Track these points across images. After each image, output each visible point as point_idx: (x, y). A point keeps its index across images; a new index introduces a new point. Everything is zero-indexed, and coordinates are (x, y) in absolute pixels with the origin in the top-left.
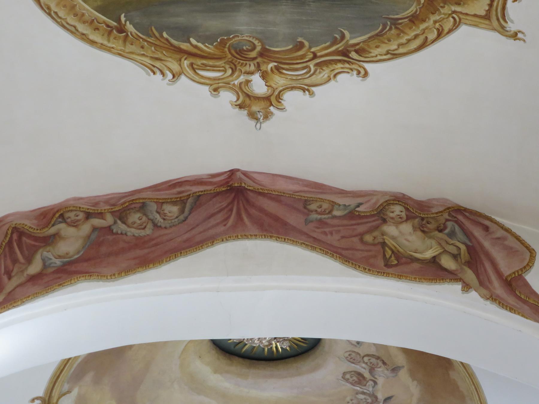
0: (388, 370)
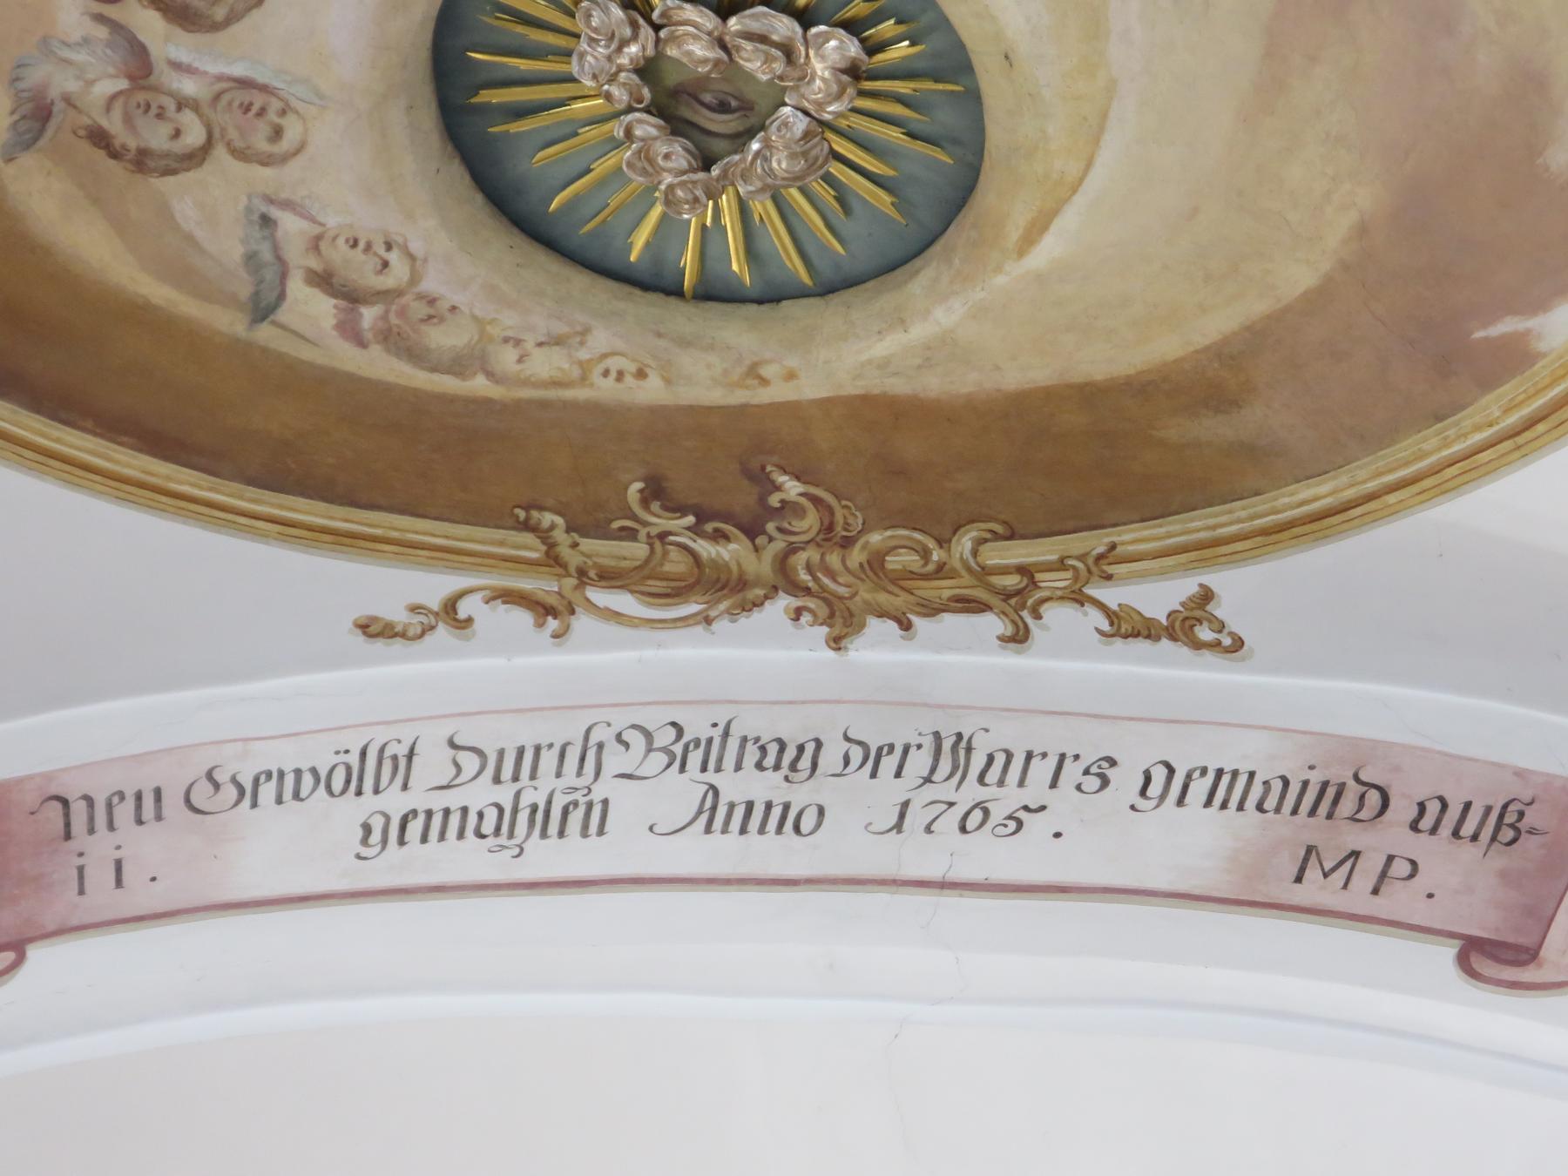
0: (68, 100)
